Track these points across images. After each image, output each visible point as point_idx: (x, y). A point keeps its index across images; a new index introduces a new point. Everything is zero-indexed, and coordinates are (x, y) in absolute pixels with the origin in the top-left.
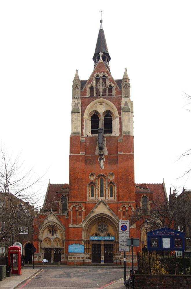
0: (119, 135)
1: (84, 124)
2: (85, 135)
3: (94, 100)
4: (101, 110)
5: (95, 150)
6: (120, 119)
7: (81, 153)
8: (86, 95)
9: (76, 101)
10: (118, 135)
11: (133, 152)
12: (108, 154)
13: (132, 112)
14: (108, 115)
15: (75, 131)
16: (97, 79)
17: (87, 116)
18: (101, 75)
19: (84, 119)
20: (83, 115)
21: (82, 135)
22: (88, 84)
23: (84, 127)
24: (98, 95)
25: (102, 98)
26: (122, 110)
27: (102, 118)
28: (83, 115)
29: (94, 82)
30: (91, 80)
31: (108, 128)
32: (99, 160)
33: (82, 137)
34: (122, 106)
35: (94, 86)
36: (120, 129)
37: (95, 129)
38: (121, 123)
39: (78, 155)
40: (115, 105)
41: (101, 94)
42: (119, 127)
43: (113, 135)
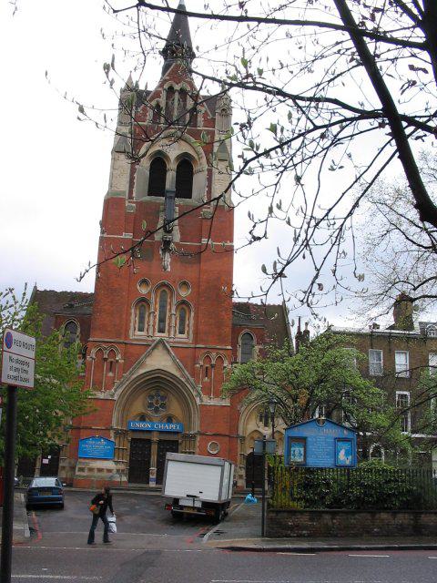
4: (173, 152)
6: (210, 173)
11: (232, 241)
14: (186, 164)
16: (171, 90)
18: (177, 87)
21: (131, 197)
22: (151, 100)
24: (170, 124)
27: (172, 166)
29: (164, 95)
30: (157, 94)
31: (184, 187)
32: (161, 252)
35: (163, 105)
37: (156, 185)
39: (118, 239)
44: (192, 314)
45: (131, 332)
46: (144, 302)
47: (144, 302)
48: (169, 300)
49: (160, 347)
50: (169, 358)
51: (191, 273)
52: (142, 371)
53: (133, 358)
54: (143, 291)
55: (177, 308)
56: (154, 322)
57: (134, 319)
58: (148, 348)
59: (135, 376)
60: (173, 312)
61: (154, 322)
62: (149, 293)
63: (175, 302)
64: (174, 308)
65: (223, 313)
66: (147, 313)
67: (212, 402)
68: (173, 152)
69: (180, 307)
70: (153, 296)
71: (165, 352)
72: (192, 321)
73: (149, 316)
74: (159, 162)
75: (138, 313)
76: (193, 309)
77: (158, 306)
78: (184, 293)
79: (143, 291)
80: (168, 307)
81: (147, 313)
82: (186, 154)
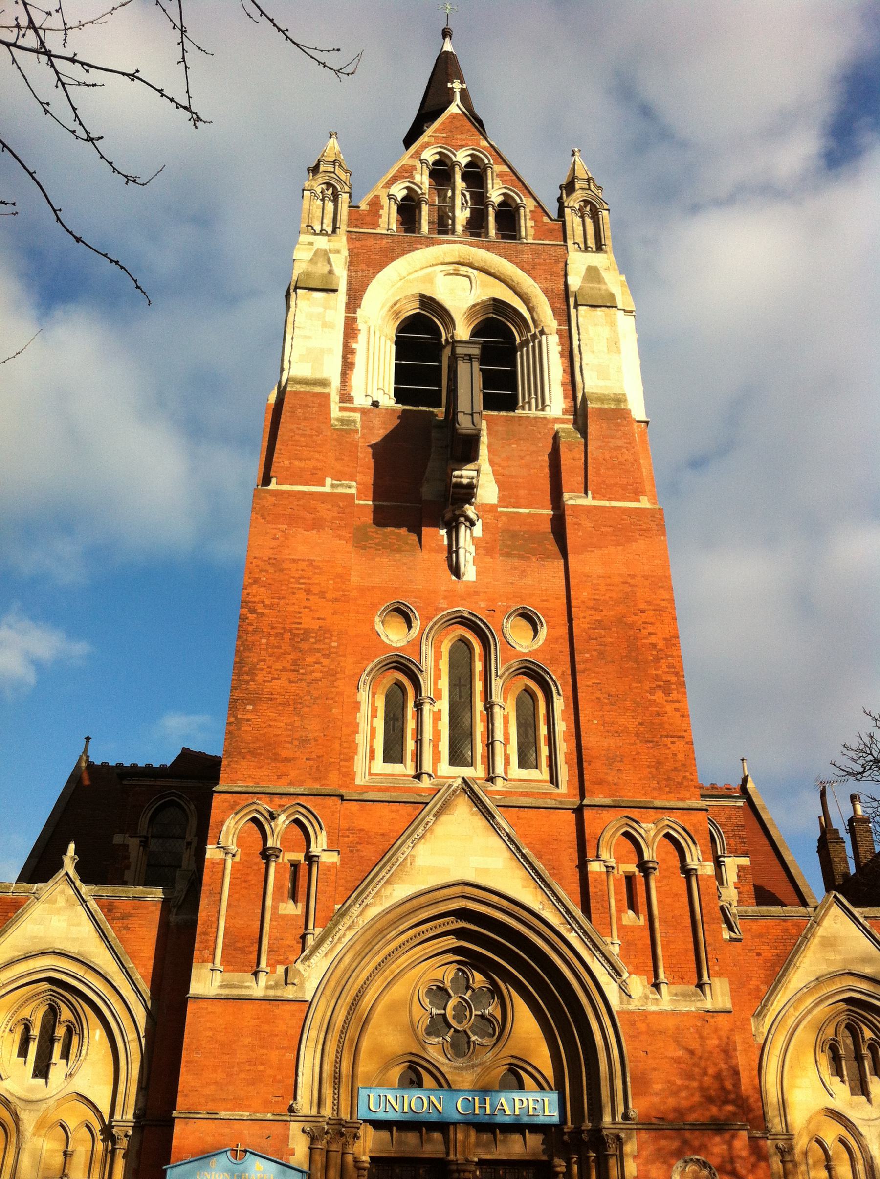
2: (361, 400)
3: (417, 249)
7: (333, 486)
8: (376, 225)
12: (501, 499)
20: (354, 302)
21: (346, 398)
23: (359, 360)
25: (461, 242)
33: (342, 409)
34: (575, 282)
36: (563, 384)
39: (311, 494)
40: (534, 278)
41: (459, 228)
44: (559, 704)
45: (360, 764)
48: (478, 666)
49: (463, 809)
50: (495, 842)
52: (400, 891)
53: (373, 858)
56: (437, 733)
57: (370, 725)
58: (418, 809)
59: (373, 912)
61: (437, 733)
62: (417, 644)
65: (659, 696)
67: (667, 1000)
71: (479, 822)
75: (380, 703)
77: (444, 684)
79: (395, 636)
80: (479, 686)
82: (497, 305)
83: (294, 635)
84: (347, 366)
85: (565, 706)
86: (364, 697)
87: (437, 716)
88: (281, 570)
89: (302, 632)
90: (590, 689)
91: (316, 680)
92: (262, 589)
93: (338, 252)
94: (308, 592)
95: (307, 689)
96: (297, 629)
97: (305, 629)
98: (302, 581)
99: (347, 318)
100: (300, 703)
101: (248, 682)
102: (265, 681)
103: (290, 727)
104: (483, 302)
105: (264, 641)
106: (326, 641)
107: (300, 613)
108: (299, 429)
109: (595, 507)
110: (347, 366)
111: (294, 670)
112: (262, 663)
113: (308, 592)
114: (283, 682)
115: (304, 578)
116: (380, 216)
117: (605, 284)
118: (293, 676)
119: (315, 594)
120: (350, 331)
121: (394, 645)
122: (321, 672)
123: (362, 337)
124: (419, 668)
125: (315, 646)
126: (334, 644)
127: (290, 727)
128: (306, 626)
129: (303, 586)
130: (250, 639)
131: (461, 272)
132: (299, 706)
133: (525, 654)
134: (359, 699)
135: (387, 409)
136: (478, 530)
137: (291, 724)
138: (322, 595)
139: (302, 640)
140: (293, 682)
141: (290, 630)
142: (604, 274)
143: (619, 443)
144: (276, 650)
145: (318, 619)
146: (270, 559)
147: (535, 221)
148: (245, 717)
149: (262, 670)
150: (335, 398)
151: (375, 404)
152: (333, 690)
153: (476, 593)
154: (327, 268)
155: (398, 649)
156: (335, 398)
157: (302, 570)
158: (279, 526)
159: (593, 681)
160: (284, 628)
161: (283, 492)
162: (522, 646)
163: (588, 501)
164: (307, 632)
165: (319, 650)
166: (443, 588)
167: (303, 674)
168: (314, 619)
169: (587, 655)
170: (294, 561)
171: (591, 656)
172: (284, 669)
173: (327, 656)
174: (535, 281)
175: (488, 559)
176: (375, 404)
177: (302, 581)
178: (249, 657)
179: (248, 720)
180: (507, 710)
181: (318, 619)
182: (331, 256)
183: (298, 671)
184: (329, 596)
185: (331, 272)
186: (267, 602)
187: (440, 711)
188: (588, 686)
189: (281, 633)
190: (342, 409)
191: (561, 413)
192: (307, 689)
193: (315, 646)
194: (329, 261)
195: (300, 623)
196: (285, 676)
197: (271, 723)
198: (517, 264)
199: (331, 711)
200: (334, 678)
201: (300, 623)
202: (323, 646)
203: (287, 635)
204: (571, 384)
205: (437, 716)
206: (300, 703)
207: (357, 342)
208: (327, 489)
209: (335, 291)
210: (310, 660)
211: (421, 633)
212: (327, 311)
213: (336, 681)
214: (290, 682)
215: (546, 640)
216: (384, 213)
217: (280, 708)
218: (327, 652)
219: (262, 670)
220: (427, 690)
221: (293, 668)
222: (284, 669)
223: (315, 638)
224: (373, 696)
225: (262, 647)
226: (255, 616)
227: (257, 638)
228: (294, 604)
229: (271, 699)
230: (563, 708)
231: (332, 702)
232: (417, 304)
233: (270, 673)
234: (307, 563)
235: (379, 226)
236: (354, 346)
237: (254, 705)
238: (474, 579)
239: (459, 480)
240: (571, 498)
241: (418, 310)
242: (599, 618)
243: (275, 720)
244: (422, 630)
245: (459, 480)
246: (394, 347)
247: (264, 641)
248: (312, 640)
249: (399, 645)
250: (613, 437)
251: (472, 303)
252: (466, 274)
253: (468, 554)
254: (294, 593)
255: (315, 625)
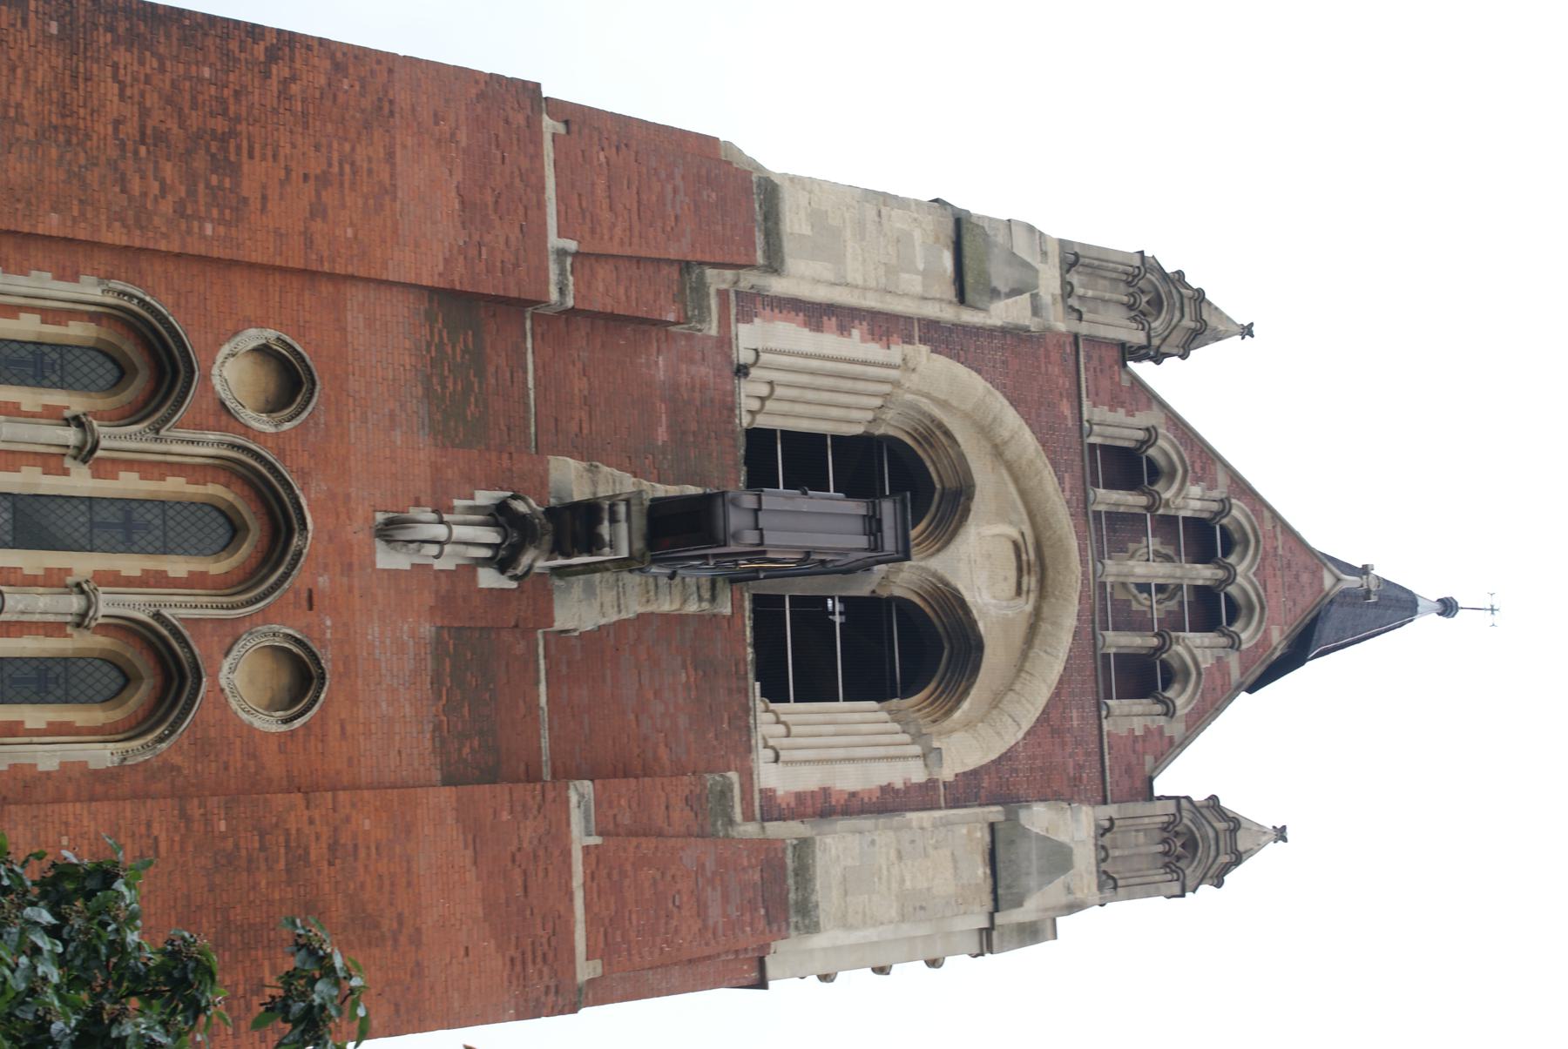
0: (761, 791)
1: (856, 345)
2: (749, 337)
3: (1061, 481)
5: (588, 452)
7: (562, 253)
9: (1049, 281)
10: (771, 777)
13: (987, 942)
15: (794, 222)
17: (944, 387)
19: (896, 352)
21: (751, 304)
23: (829, 342)
25: (1084, 574)
26: (995, 813)
28: (937, 335)
32: (485, 498)
33: (723, 295)
34: (1039, 818)
36: (826, 791)
38: (888, 803)
42: (848, 780)
43: (760, 705)
44: (102, 755)
46: (152, 368)
47: (152, 368)
48: (178, 566)
51: (388, 698)
54: (232, 374)
55: (127, 628)
60: (108, 604)
63: (180, 608)
64: (136, 606)
66: (75, 403)
68: (975, 566)
69: (142, 662)
70: (209, 445)
72: (47, 758)
73: (55, 415)
74: (901, 477)
75: (77, 331)
76: (137, 750)
77: (129, 484)
78: (240, 680)
79: (232, 374)
80: (130, 565)
81: (75, 403)
83: (224, 139)
84: (815, 314)
85: (96, 772)
86: (90, 290)
87: (51, 462)
88: (367, 125)
89: (233, 158)
90: (143, 830)
91: (123, 180)
92: (323, 81)
93: (1036, 310)
94: (323, 180)
95: (103, 158)
96: (239, 147)
97: (240, 165)
98: (347, 168)
99: (908, 319)
100: (68, 142)
101: (111, 28)
102: (115, 66)
103: (12, 113)
104: (974, 623)
105: (207, 72)
106: (215, 213)
107: (275, 157)
108: (675, 191)
109: (567, 854)
110: (815, 314)
111: (143, 134)
112: (155, 65)
113: (323, 180)
114: (114, 107)
115: (354, 173)
116: (1112, 409)
117: (1040, 887)
118: (130, 129)
119: (318, 195)
120: (884, 325)
121: (215, 371)
122: (145, 194)
123: (874, 351)
124: (166, 420)
125: (201, 186)
126: (208, 229)
127: (12, 113)
128: (246, 168)
129: (336, 169)
130: (209, 42)
131: (1025, 579)
132: (61, 138)
133: (214, 677)
134: (83, 278)
135: (733, 393)
136: (489, 579)
137: (19, 119)
138: (317, 211)
139: (213, 156)
140: (116, 130)
141: (233, 133)
142: (1060, 882)
143: (714, 912)
144: (187, 96)
145: (264, 198)
146: (391, 102)
147: (1144, 738)
148: (32, 15)
149: (142, 63)
150: (749, 280)
151: (742, 371)
152: (103, 217)
153: (348, 568)
154: (1003, 289)
155: (207, 377)
156: (749, 280)
157: (370, 171)
158: (464, 129)
159: (163, 837)
160: (238, 119)
161: (538, 144)
162: (232, 670)
163: (580, 837)
164: (234, 170)
165: (192, 192)
166: (353, 491)
167: (136, 153)
168: (264, 187)
169: (223, 826)
170: (390, 156)
171: (223, 837)
172: (144, 112)
173: (180, 210)
174: (1028, 733)
175: (429, 599)
176: (742, 371)
177: (347, 168)
178: (168, 36)
179: (25, 22)
180: (76, 633)
181: (264, 198)
182: (1027, 296)
183: (143, 142)
184: (318, 225)
185: (995, 294)
186: (295, 88)
187: (66, 472)
188: (149, 825)
189: (225, 113)
190: (723, 295)
191: (763, 786)
192: (103, 158)
193: (201, 186)
194: (1015, 292)
195: (251, 157)
196: (130, 111)
197: (19, 71)
198: (1057, 694)
199: (54, 209)
200: (131, 222)
201: (251, 157)
202: (202, 201)
203: (220, 125)
204: (824, 807)
205: (51, 462)
206: (68, 142)
207: (863, 340)
208: (554, 241)
209: (961, 298)
210: (168, 169)
211: (246, 430)
212: (919, 278)
213: (124, 226)
214: (117, 123)
215: (251, 728)
216: (1120, 415)
217: (55, 95)
218: (189, 212)
219: (142, 63)
220: (114, 439)
221: (149, 132)
222: (144, 112)
223: (221, 187)
224: (94, 318)
225: (194, 68)
226: (262, 58)
227: (212, 58)
228: (294, 146)
229: (74, 77)
230: (92, 766)
231: (75, 213)
232: (951, 483)
233: (135, 79)
234: (387, 181)
235: (1095, 405)
236: (856, 333)
237: (60, 39)
238: (380, 565)
239: (606, 516)
240: (582, 796)
241: (938, 486)
242: (313, 857)
243: (27, 81)
244: (257, 436)
245: (606, 516)
246: (858, 430)
247: (207, 72)
248: (214, 179)
249: (216, 382)
250: (726, 898)
251: (968, 597)
252: (1025, 587)
253: (434, 549)
254: (317, 148)
255: (249, 188)
